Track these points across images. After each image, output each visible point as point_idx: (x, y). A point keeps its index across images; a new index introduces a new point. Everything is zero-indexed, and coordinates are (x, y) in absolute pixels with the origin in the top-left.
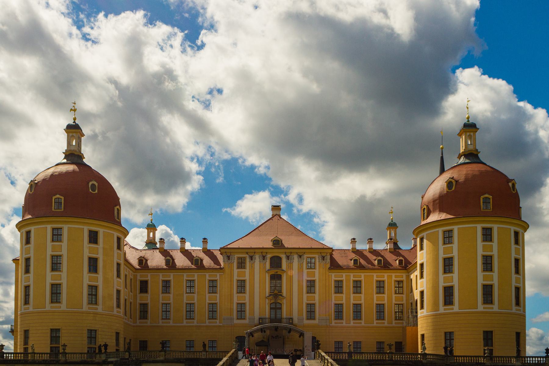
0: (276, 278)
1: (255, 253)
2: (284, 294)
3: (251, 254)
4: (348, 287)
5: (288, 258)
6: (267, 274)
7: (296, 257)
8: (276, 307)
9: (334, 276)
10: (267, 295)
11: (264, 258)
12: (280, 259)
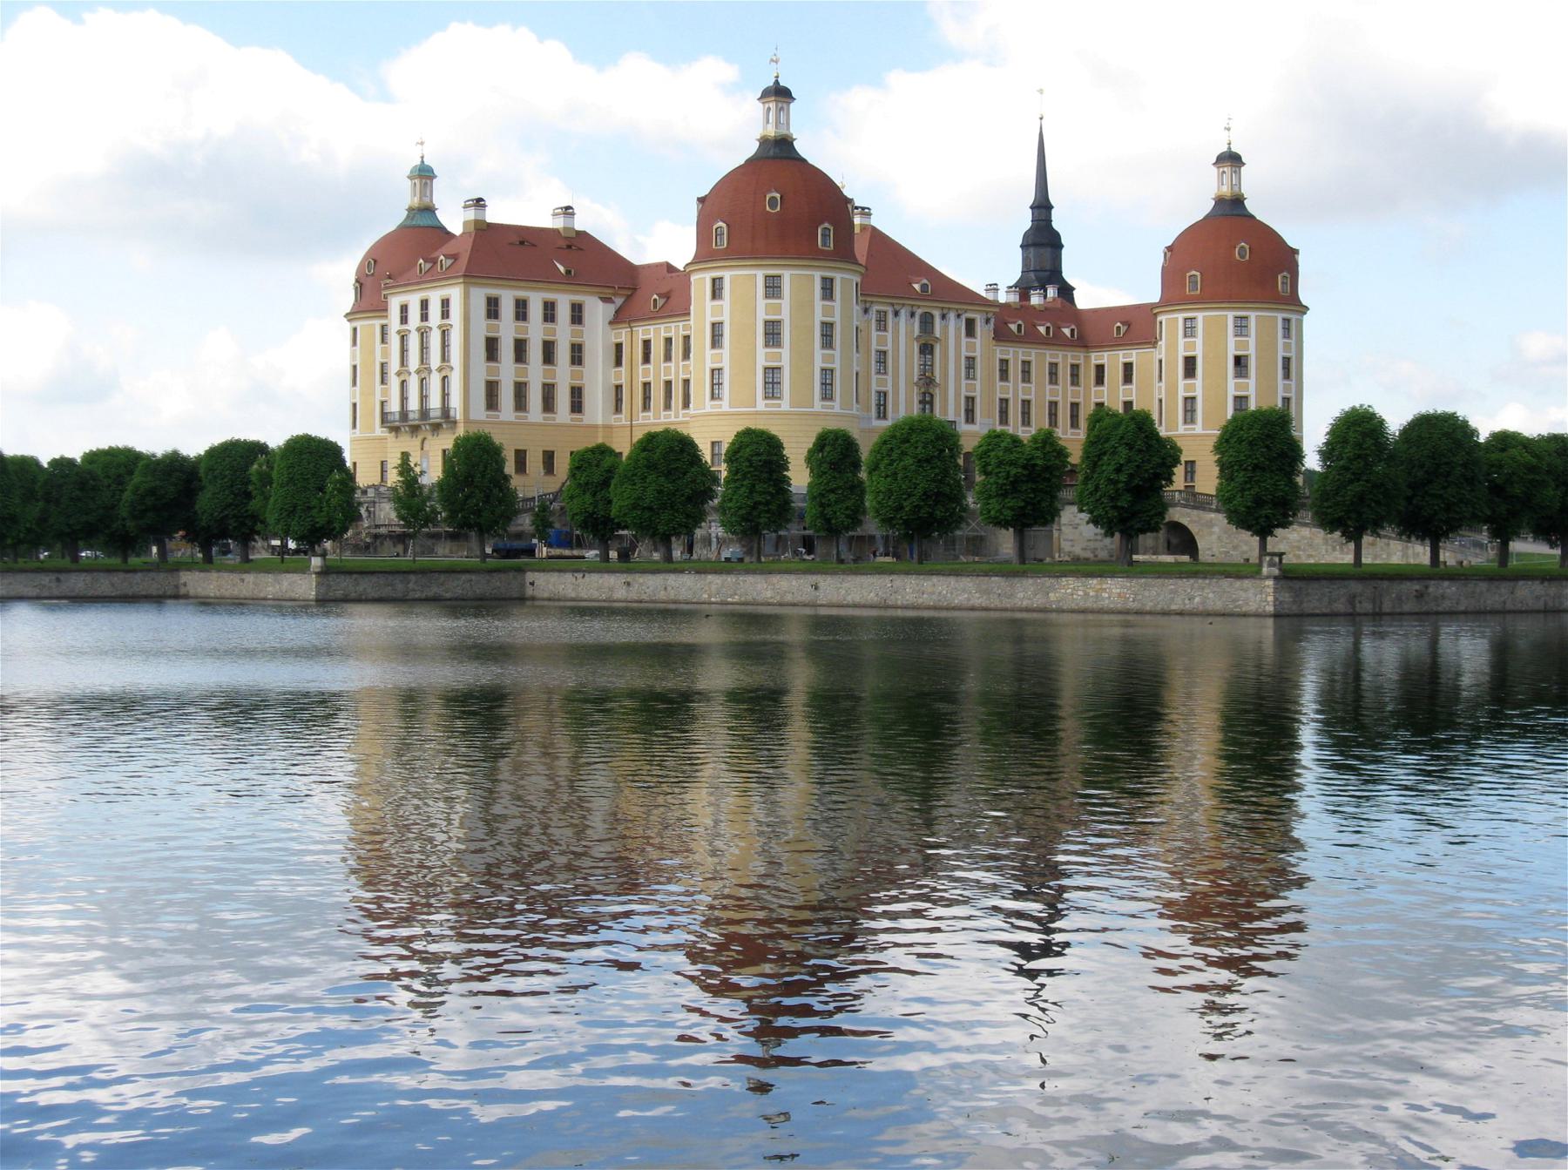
0: (926, 349)
1: (904, 305)
2: (937, 380)
3: (897, 308)
4: (1015, 370)
5: (943, 317)
6: (915, 344)
7: (952, 316)
8: (927, 401)
9: (1000, 352)
10: (916, 379)
11: (913, 315)
12: (932, 316)
